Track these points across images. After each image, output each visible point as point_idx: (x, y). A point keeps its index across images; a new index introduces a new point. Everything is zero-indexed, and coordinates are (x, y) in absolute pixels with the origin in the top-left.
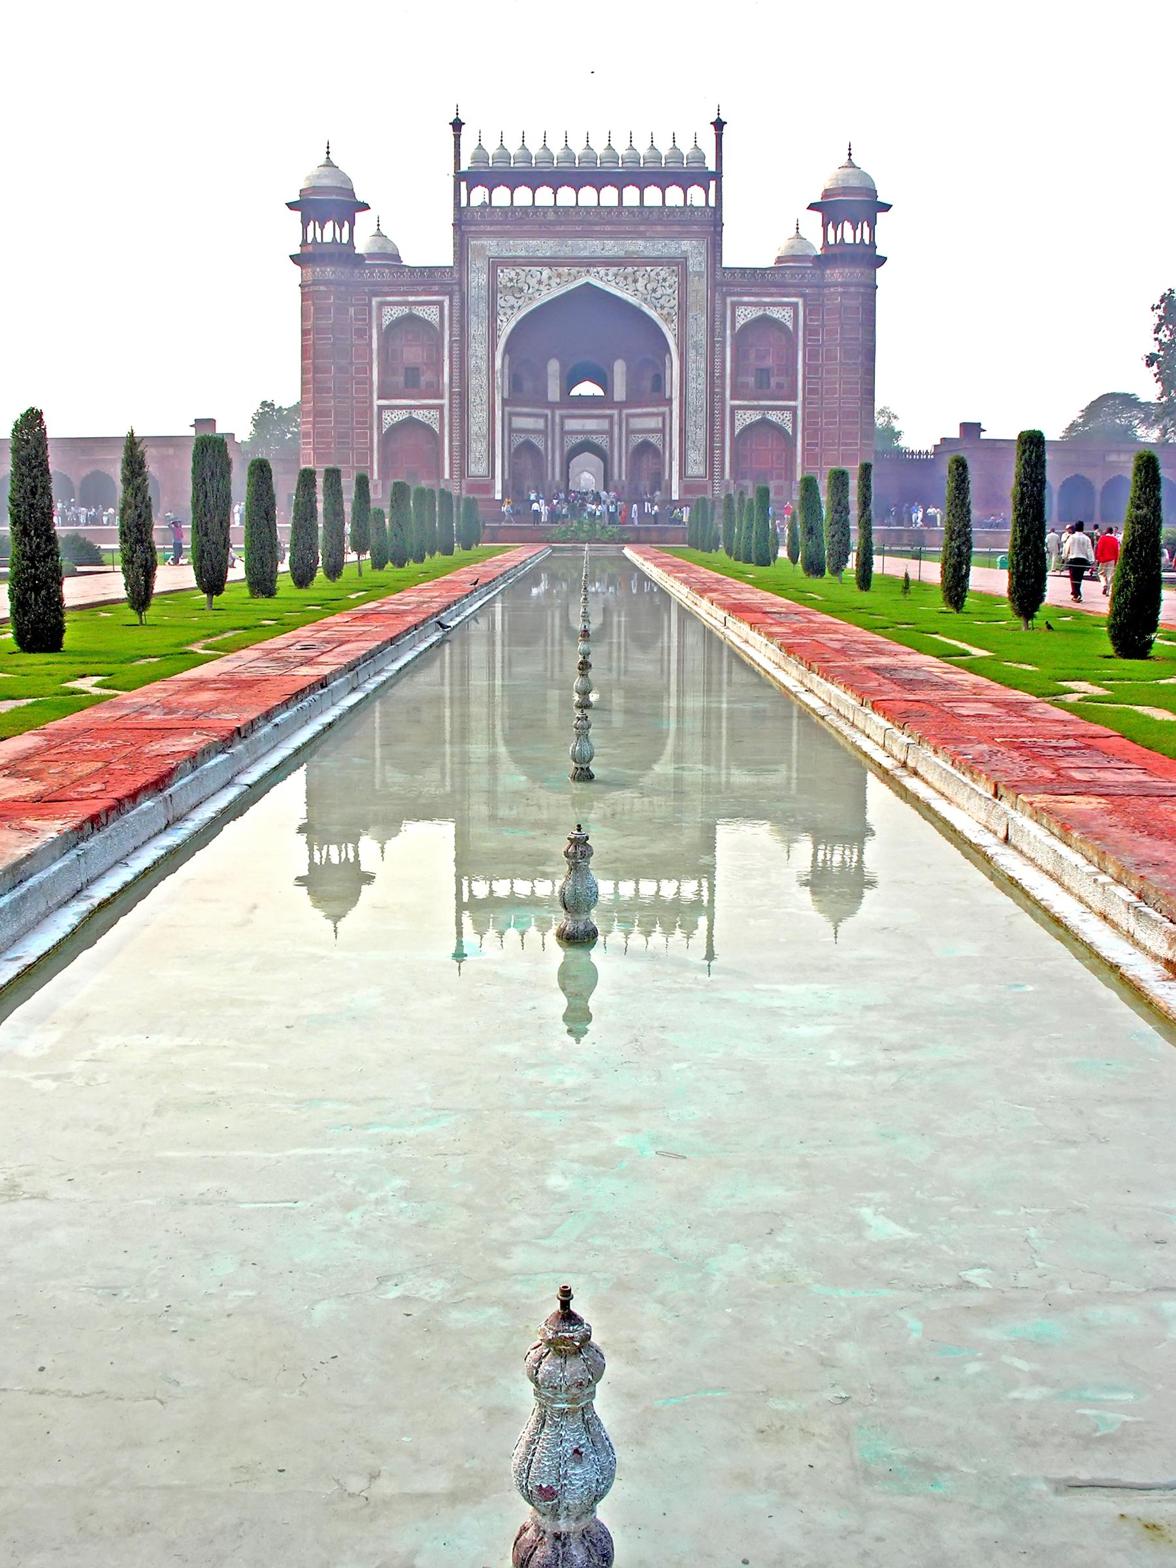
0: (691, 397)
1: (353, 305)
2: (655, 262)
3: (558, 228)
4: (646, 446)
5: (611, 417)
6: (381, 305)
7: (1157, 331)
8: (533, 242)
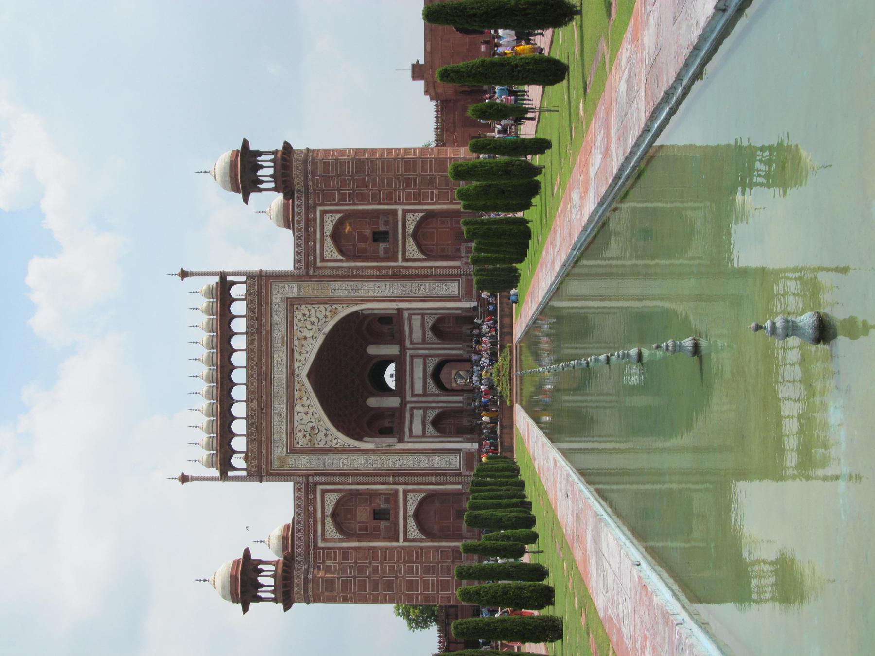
0: (396, 293)
1: (324, 562)
2: (290, 324)
3: (264, 399)
4: (435, 329)
5: (412, 357)
6: (324, 539)
8: (276, 419)
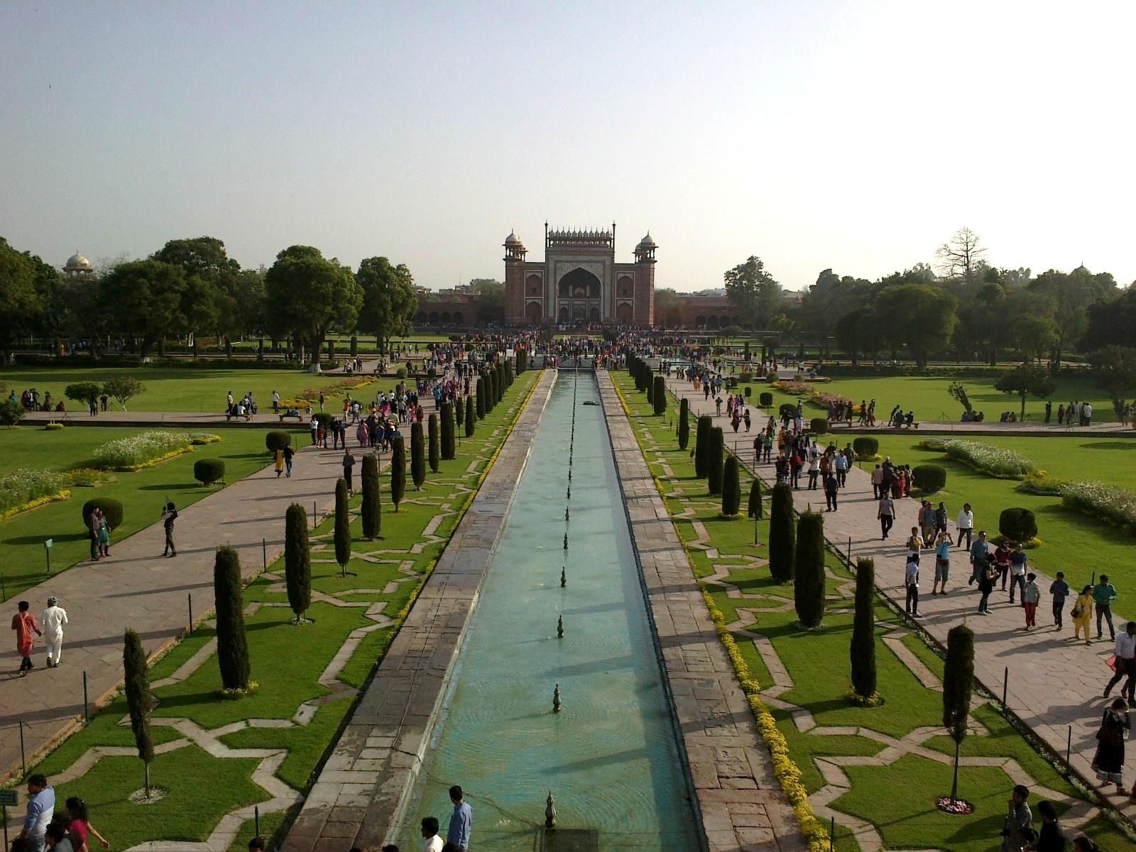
2: (597, 262)
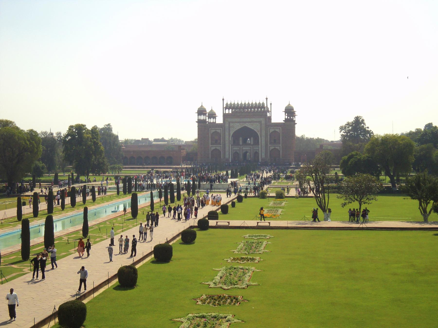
2: (256, 122)
6: (211, 130)
7: (340, 132)
